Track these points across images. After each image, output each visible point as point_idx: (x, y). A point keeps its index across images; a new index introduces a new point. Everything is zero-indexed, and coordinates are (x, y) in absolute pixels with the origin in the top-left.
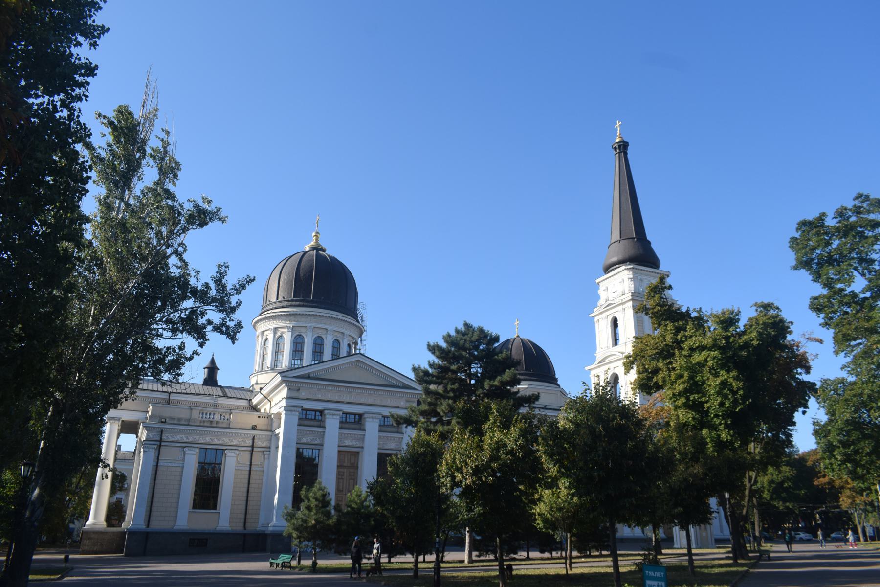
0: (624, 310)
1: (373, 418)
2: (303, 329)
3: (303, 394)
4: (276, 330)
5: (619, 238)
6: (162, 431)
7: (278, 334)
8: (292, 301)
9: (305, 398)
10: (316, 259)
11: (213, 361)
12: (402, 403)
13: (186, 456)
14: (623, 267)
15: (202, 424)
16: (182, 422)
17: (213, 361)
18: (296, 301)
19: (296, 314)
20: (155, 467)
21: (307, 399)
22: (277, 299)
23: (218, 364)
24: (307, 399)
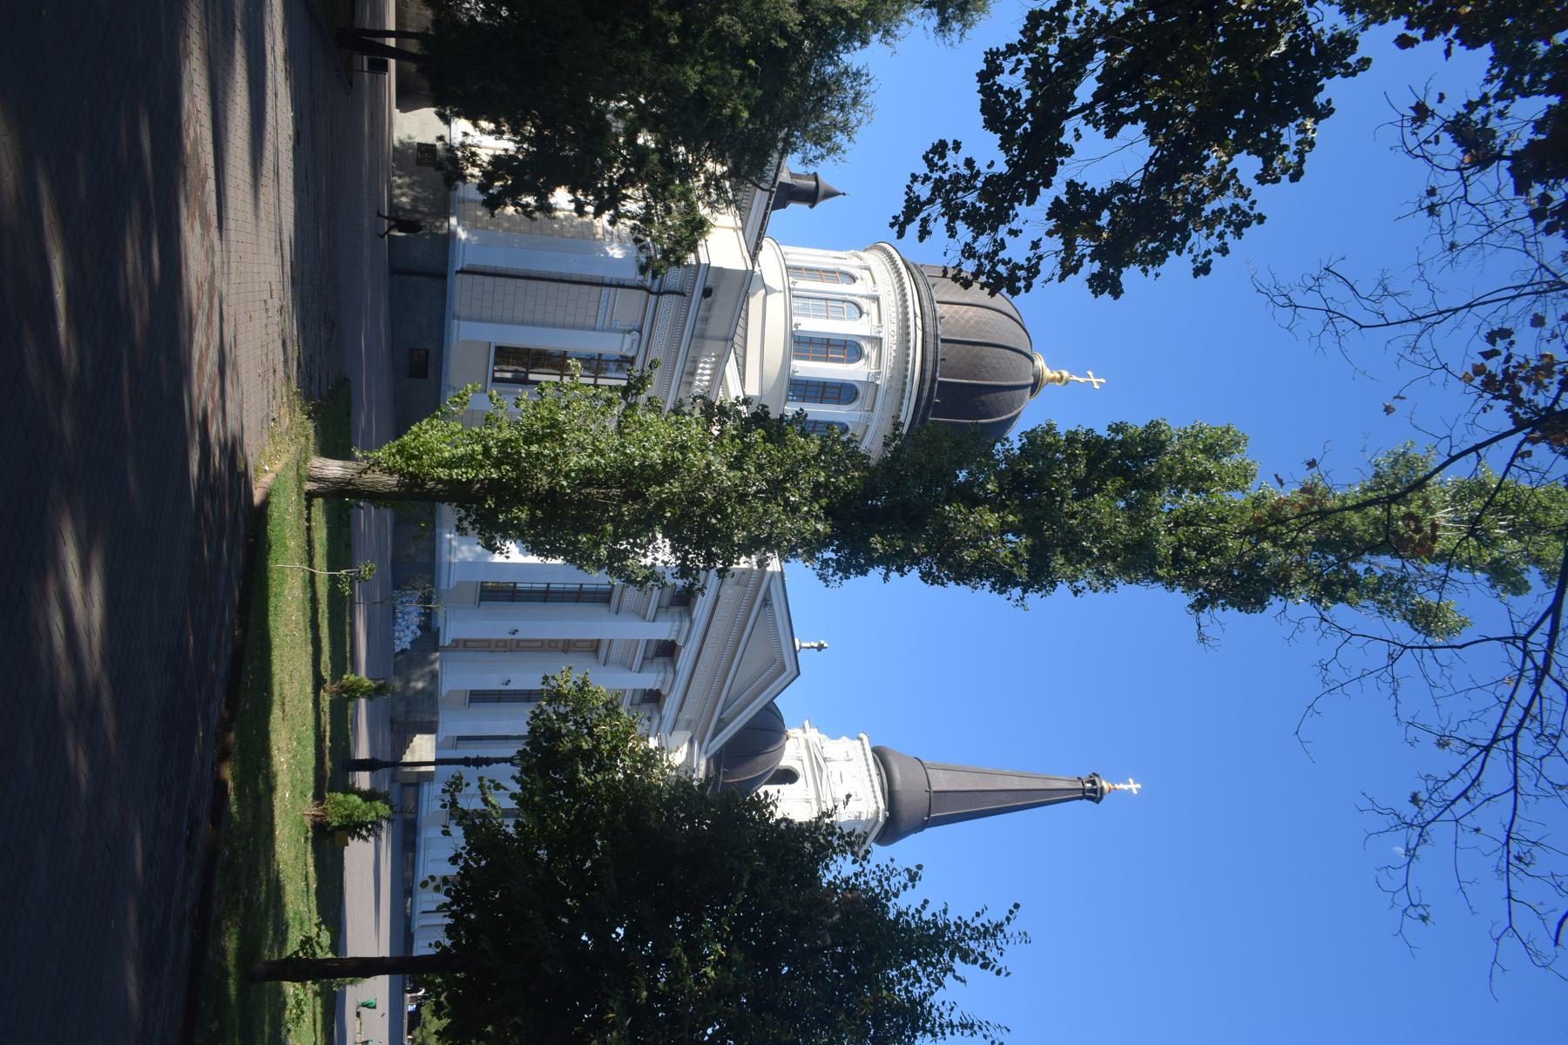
0: (808, 801)
1: (663, 682)
2: (868, 401)
3: (729, 591)
4: (877, 341)
5: (934, 788)
6: (682, 294)
7: (866, 305)
8: (933, 380)
9: (721, 594)
10: (1003, 421)
11: (831, 194)
12: (687, 716)
13: (621, 335)
14: (882, 806)
15: (689, 359)
16: (698, 325)
17: (831, 194)
18: (932, 388)
19: (903, 397)
20: (600, 281)
21: (718, 597)
22: (943, 341)
23: (822, 205)
24: (718, 597)
